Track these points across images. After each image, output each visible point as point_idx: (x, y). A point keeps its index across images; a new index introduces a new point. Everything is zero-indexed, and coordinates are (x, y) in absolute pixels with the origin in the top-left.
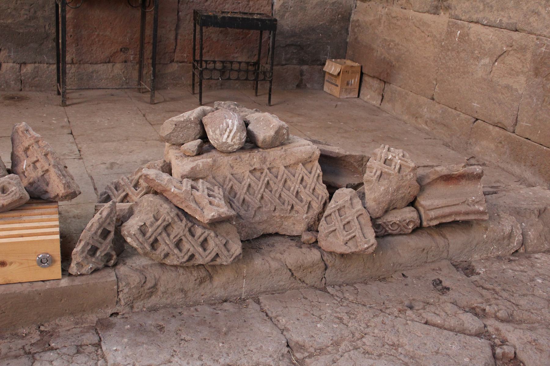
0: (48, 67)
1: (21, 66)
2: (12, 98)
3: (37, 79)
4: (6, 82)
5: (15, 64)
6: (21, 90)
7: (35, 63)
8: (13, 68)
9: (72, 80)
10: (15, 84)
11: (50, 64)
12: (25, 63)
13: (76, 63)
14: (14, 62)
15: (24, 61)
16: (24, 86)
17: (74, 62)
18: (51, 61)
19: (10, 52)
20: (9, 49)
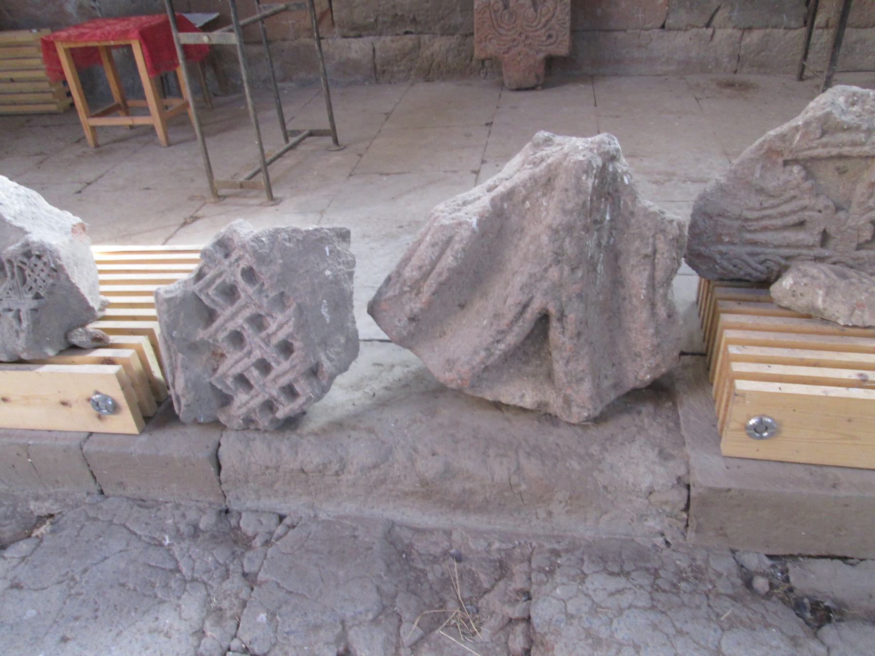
0: (785, 34)
1: (743, 34)
2: (730, 85)
3: (763, 54)
4: (717, 59)
5: (735, 31)
6: (735, 72)
7: (767, 27)
8: (731, 36)
9: (819, 55)
10: (729, 62)
11: (790, 29)
12: (750, 29)
13: (832, 27)
14: (734, 28)
15: (751, 24)
16: (742, 66)
17: (830, 24)
18: (793, 24)
19: (732, 11)
20: (732, 5)
